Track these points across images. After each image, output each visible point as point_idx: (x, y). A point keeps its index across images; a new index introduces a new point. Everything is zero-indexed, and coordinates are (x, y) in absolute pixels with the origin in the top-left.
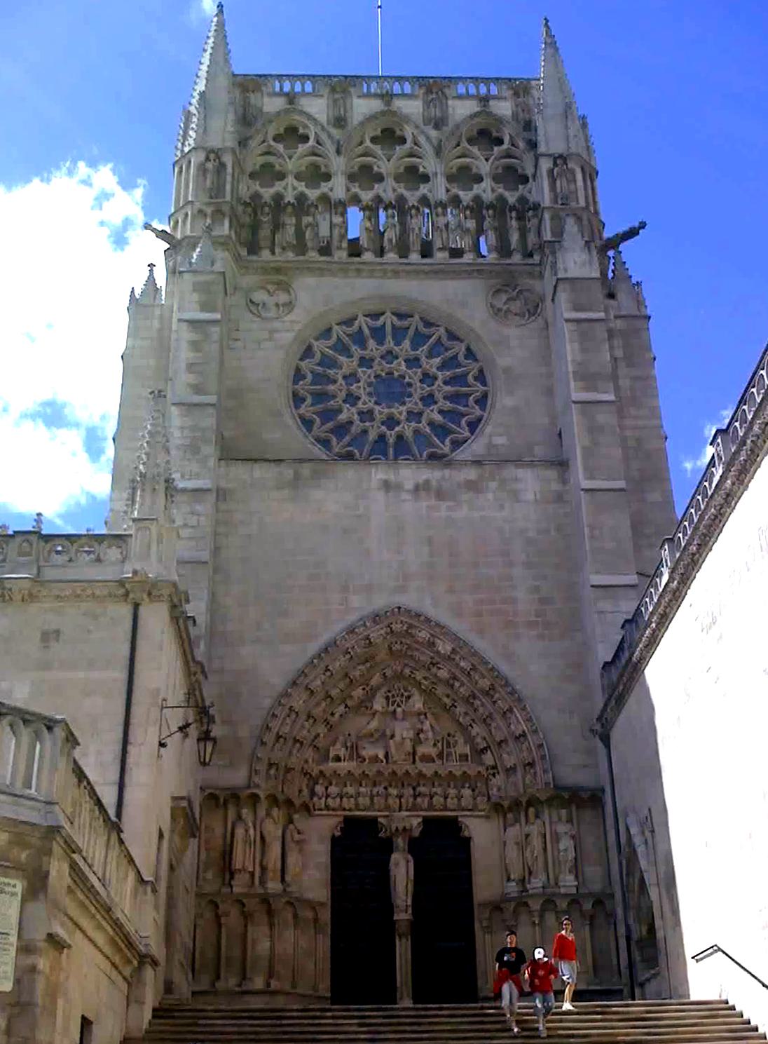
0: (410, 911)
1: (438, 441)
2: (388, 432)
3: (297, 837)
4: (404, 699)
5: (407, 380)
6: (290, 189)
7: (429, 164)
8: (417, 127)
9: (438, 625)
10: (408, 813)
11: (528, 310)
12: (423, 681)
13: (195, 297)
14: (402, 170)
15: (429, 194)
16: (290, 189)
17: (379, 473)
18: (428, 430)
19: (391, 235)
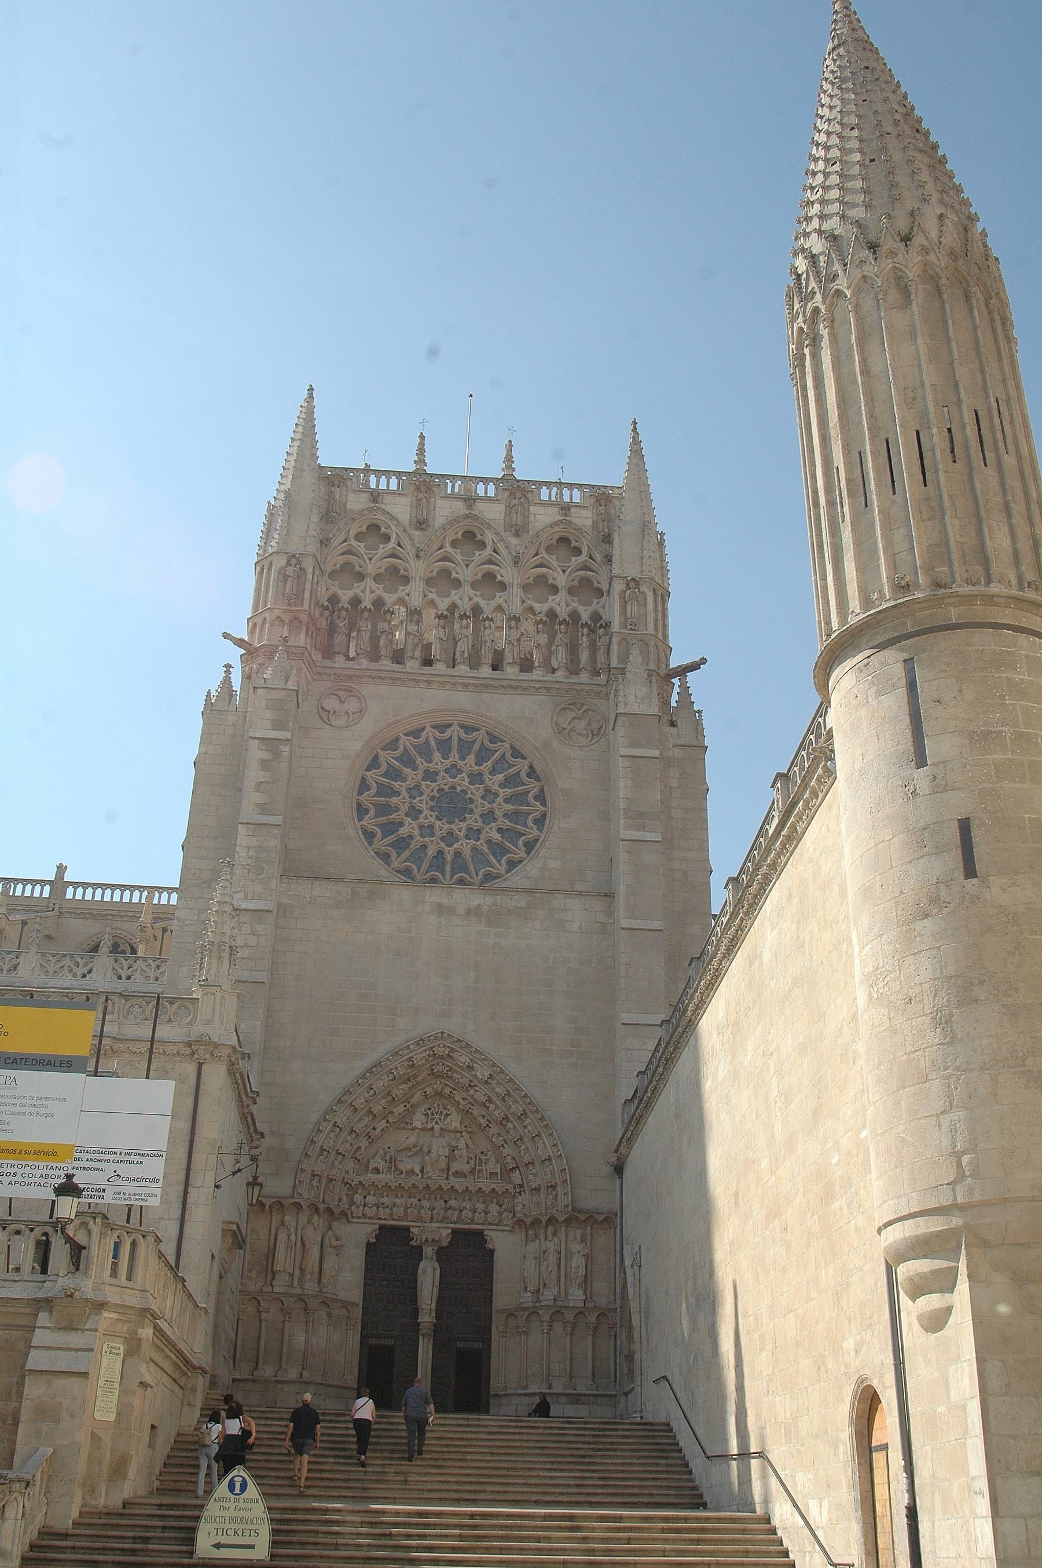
0: (434, 1314)
1: (495, 861)
2: (446, 848)
3: (334, 1243)
4: (442, 1118)
5: (469, 795)
6: (368, 591)
7: (507, 573)
8: (497, 534)
9: (477, 1051)
10: (437, 1225)
11: (592, 731)
12: (461, 1101)
13: (268, 714)
14: (479, 576)
15: (505, 604)
16: (369, 591)
17: (434, 896)
18: (485, 848)
19: (463, 647)
